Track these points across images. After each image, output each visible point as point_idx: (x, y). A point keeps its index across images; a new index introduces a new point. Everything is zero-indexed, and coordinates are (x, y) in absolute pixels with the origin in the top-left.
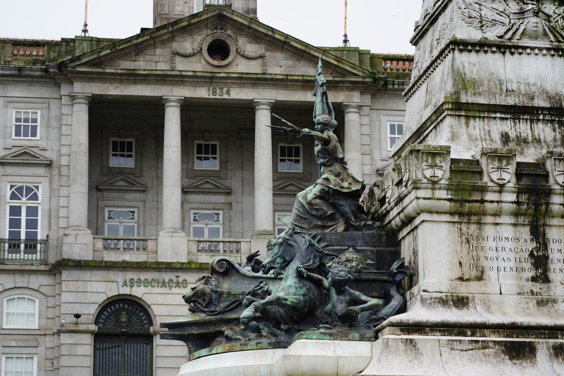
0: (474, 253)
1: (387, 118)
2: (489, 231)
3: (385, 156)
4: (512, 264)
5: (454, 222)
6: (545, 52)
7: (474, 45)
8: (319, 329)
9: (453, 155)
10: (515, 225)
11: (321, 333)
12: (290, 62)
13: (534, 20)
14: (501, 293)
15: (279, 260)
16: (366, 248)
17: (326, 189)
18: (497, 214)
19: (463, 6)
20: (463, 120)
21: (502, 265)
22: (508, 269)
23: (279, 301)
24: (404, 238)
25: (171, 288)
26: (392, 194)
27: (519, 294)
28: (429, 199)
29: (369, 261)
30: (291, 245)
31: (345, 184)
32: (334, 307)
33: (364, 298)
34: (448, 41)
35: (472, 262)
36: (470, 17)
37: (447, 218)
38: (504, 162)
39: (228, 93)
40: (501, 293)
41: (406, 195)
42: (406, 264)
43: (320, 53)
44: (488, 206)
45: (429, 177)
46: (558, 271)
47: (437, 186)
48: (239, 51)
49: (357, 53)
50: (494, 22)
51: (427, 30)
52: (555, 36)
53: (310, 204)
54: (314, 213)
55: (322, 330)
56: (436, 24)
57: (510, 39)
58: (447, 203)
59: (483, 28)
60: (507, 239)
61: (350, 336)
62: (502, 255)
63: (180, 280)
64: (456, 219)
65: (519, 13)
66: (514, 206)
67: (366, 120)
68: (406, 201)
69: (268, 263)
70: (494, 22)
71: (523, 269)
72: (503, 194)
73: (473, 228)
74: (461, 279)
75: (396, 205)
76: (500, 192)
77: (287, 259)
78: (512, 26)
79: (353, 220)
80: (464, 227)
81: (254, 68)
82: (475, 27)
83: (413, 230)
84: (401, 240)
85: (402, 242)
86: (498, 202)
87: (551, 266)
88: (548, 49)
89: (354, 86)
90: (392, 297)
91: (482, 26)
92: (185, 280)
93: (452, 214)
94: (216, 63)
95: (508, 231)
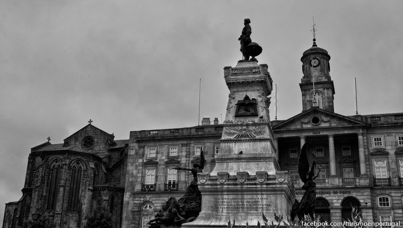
1: (373, 136)
3: (373, 149)
7: (226, 141)
12: (338, 122)
21: (224, 206)
22: (225, 208)
39: (319, 133)
43: (347, 118)
45: (201, 182)
48: (322, 120)
49: (360, 117)
65: (240, 130)
67: (365, 138)
70: (234, 134)
81: (327, 125)
88: (249, 140)
89: (360, 127)
94: (314, 124)
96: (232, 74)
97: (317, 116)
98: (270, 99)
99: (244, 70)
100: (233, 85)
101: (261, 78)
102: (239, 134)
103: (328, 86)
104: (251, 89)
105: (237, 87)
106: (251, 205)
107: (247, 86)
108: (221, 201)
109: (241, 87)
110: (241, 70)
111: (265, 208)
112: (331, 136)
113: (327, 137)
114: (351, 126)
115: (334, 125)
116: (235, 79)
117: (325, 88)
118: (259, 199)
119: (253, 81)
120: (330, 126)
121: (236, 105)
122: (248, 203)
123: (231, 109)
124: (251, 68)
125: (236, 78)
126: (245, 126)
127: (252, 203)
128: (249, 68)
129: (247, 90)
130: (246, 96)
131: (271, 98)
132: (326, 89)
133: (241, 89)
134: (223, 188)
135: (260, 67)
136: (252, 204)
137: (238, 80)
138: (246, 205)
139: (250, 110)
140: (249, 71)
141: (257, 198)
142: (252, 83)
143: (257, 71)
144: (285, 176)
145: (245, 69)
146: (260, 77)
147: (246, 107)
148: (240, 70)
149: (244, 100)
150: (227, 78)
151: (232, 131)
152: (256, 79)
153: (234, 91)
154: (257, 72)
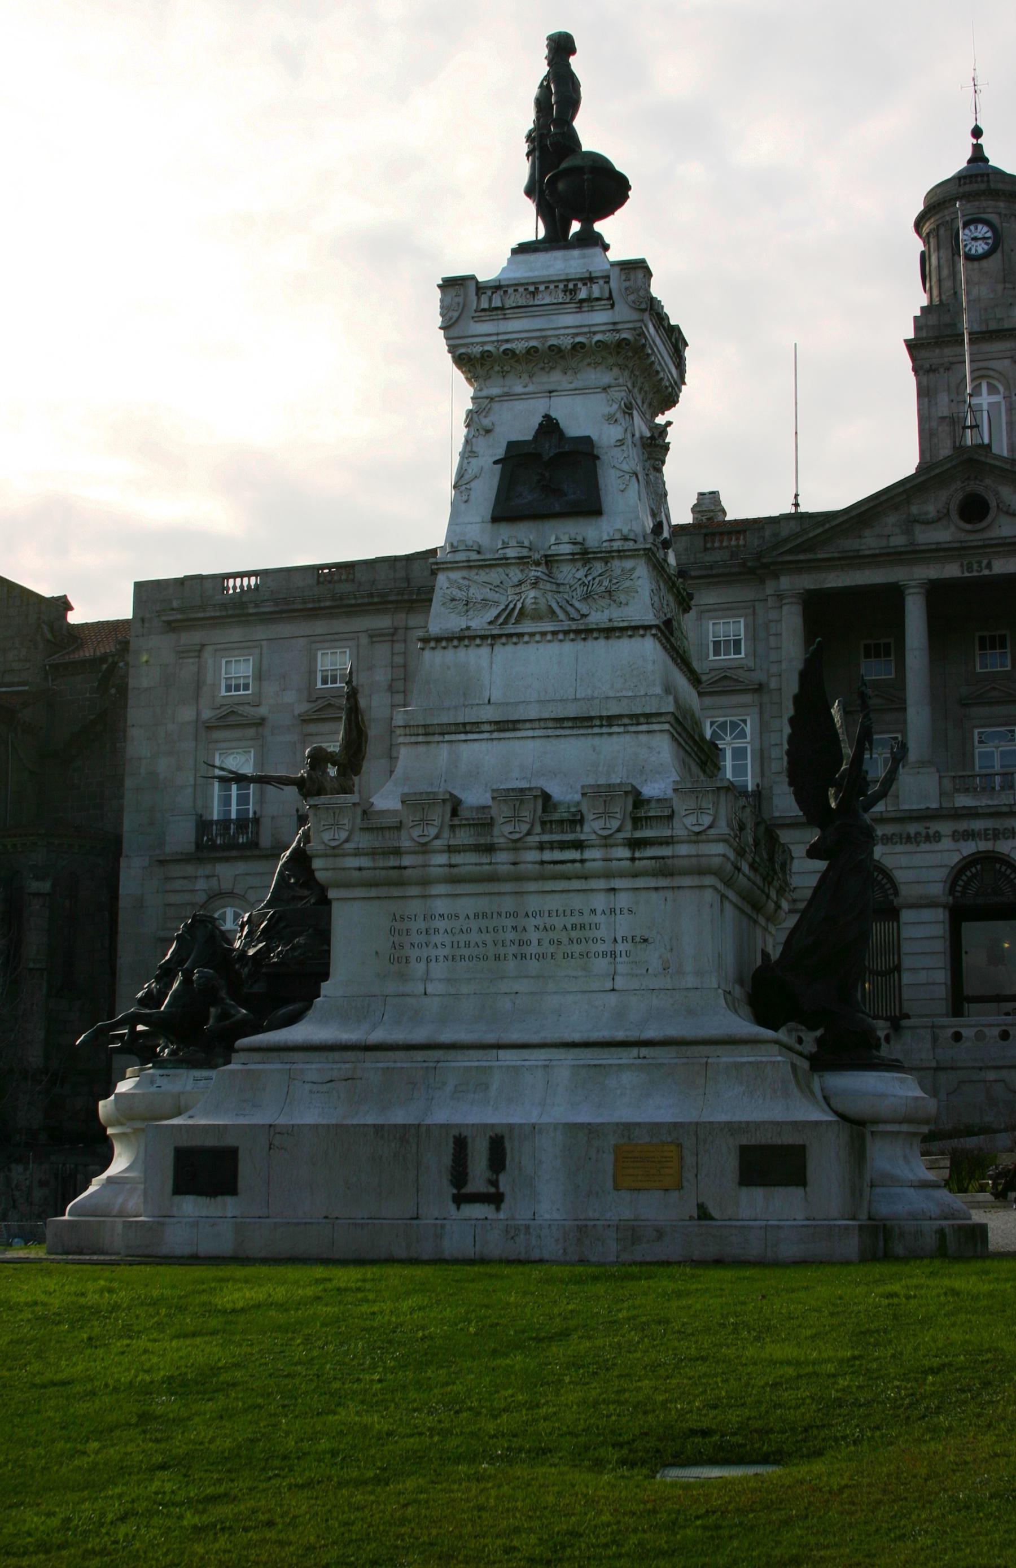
7: (449, 639)
13: (532, 594)
14: (425, 994)
18: (425, 882)
21: (434, 953)
22: (441, 959)
25: (918, 844)
36: (453, 600)
40: (425, 994)
45: (326, 841)
46: (510, 957)
50: (486, 603)
52: (566, 612)
59: (471, 613)
60: (442, 916)
62: (438, 939)
63: (931, 832)
65: (517, 586)
70: (486, 603)
78: (507, 606)
82: (459, 613)
86: (424, 866)
88: (554, 633)
92: (937, 832)
96: (476, 311)
98: (668, 429)
99: (537, 289)
101: (618, 331)
102: (511, 606)
104: (572, 386)
105: (504, 374)
106: (560, 943)
107: (551, 368)
108: (423, 925)
109: (525, 376)
110: (521, 289)
111: (624, 953)
116: (494, 338)
118: (599, 911)
119: (578, 347)
121: (500, 466)
124: (568, 280)
125: (498, 334)
126: (537, 564)
127: (564, 933)
128: (560, 281)
129: (551, 388)
130: (547, 417)
131: (669, 424)
133: (525, 387)
134: (429, 866)
135: (615, 274)
136: (565, 941)
137: (507, 341)
138: (535, 942)
140: (561, 295)
141: (586, 912)
143: (596, 294)
144: (716, 804)
145: (542, 288)
146: (614, 324)
147: (547, 475)
148: (516, 291)
149: (536, 437)
151: (477, 593)
152: (595, 333)
153: (487, 398)
154: (598, 299)
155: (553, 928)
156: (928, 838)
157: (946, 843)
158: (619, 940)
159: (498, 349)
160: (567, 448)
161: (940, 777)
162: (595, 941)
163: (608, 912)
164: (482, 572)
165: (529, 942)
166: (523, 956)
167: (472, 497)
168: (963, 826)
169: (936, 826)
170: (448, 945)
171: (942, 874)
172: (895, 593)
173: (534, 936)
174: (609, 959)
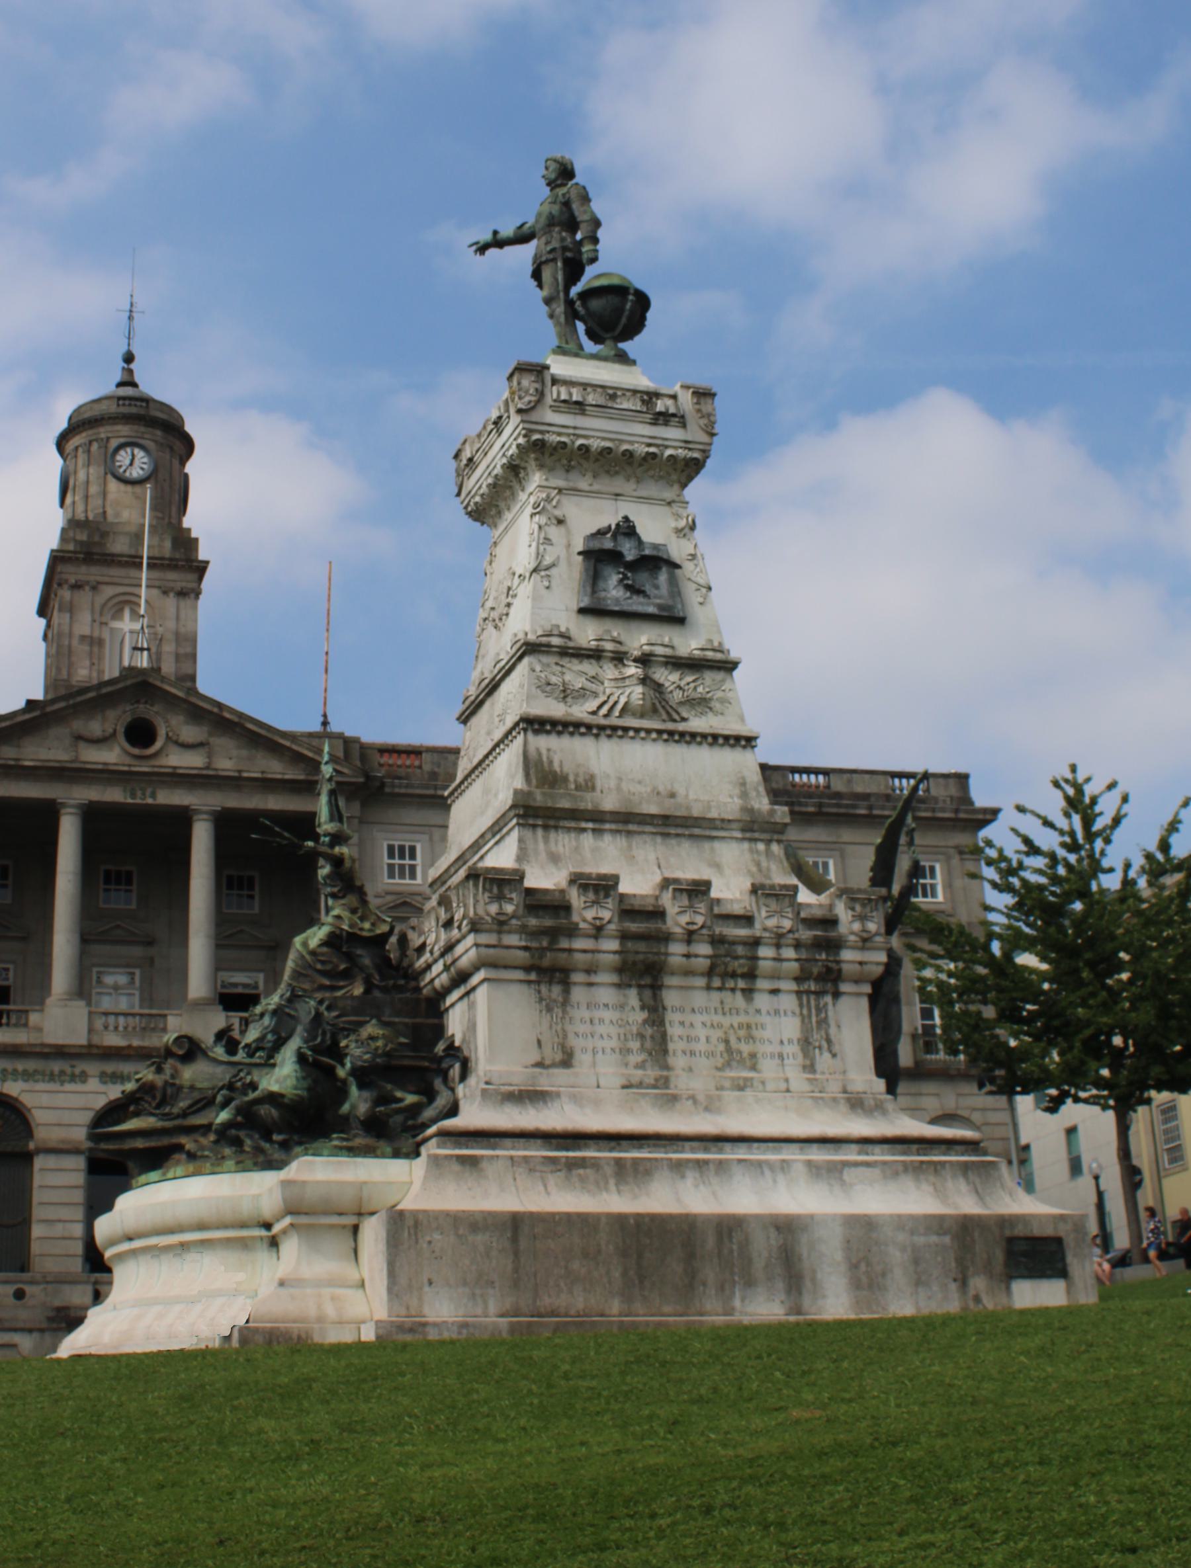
0: (559, 1027)
2: (578, 994)
4: (614, 1043)
5: (529, 982)
6: (654, 735)
8: (331, 1140)
9: (529, 883)
10: (619, 986)
11: (336, 1147)
12: (244, 753)
15: (270, 1037)
16: (397, 1020)
17: (338, 932)
19: (538, 668)
20: (540, 832)
21: (600, 1044)
22: (608, 1051)
23: (273, 1098)
24: (453, 1005)
25: (62, 1083)
26: (437, 940)
27: (624, 1087)
28: (494, 946)
29: (403, 1040)
30: (289, 1015)
31: (367, 925)
32: (354, 1107)
33: (399, 1094)
34: (517, 718)
35: (556, 1039)
36: (549, 684)
37: (519, 975)
38: (602, 894)
39: (153, 796)
40: (598, 1087)
41: (458, 941)
42: (457, 1044)
44: (579, 957)
47: (506, 928)
49: (341, 741)
51: (482, 703)
52: (668, 713)
53: (313, 953)
54: (319, 966)
55: (336, 1143)
56: (496, 694)
57: (606, 716)
58: (521, 954)
59: (569, 699)
60: (606, 1006)
61: (379, 1152)
62: (601, 1029)
63: (77, 1071)
64: (533, 976)
66: (617, 957)
68: (459, 950)
69: (254, 1041)
71: (629, 1051)
72: (600, 941)
73: (556, 990)
74: (540, 1064)
75: (442, 955)
76: (596, 937)
77: (283, 1035)
79: (377, 977)
80: (544, 989)
82: (556, 698)
83: (467, 994)
84: (447, 1010)
85: (451, 1012)
86: (593, 951)
87: (671, 1046)
88: (660, 732)
90: (438, 1092)
91: (565, 697)
93: (527, 969)
94: (136, 751)
95: (606, 995)
97: (152, 712)
100: (551, 455)
101: (690, 449)
103: (184, 584)
104: (635, 494)
105: (568, 469)
107: (617, 473)
109: (589, 475)
112: (205, 816)
113: (182, 819)
114: (302, 777)
115: (225, 764)
116: (571, 431)
117: (172, 589)
118: (764, 1011)
120: (207, 768)
122: (711, 1032)
123: (553, 571)
125: (575, 428)
128: (628, 390)
130: (626, 519)
132: (172, 595)
134: (599, 951)
138: (703, 1039)
139: (648, 588)
142: (640, 465)
146: (686, 442)
147: (629, 575)
150: (534, 416)
155: (720, 1026)
156: (73, 1078)
157: (93, 1084)
158: (786, 1042)
159: (573, 443)
160: (647, 552)
161: (90, 1013)
162: (762, 1041)
163: (772, 1012)
164: (575, 661)
165: (697, 1039)
166: (692, 1053)
167: (554, 584)
168: (110, 1067)
169: (81, 1066)
170: (615, 1038)
171: (87, 1117)
172: (49, 813)
173: (702, 1033)
174: (777, 1061)
